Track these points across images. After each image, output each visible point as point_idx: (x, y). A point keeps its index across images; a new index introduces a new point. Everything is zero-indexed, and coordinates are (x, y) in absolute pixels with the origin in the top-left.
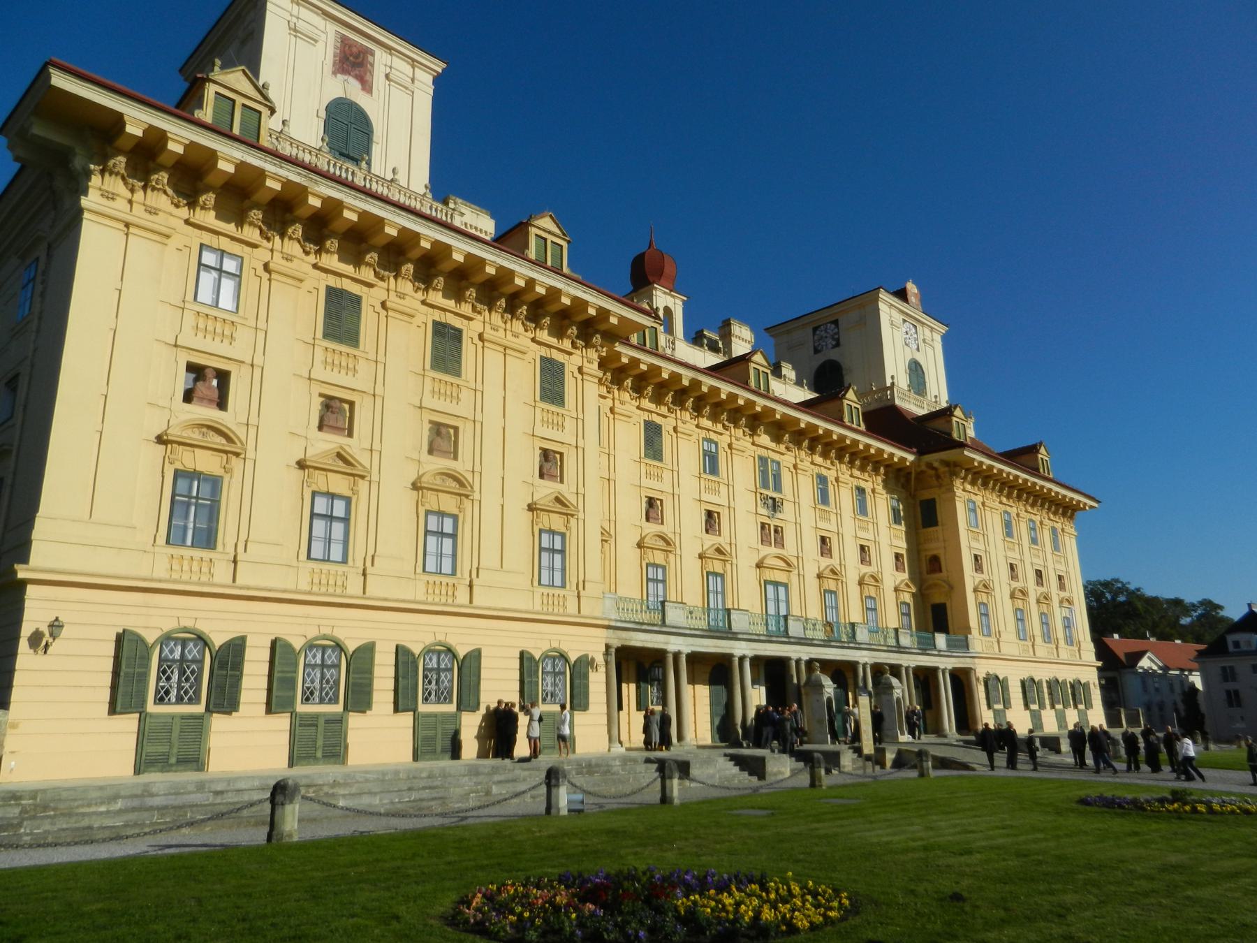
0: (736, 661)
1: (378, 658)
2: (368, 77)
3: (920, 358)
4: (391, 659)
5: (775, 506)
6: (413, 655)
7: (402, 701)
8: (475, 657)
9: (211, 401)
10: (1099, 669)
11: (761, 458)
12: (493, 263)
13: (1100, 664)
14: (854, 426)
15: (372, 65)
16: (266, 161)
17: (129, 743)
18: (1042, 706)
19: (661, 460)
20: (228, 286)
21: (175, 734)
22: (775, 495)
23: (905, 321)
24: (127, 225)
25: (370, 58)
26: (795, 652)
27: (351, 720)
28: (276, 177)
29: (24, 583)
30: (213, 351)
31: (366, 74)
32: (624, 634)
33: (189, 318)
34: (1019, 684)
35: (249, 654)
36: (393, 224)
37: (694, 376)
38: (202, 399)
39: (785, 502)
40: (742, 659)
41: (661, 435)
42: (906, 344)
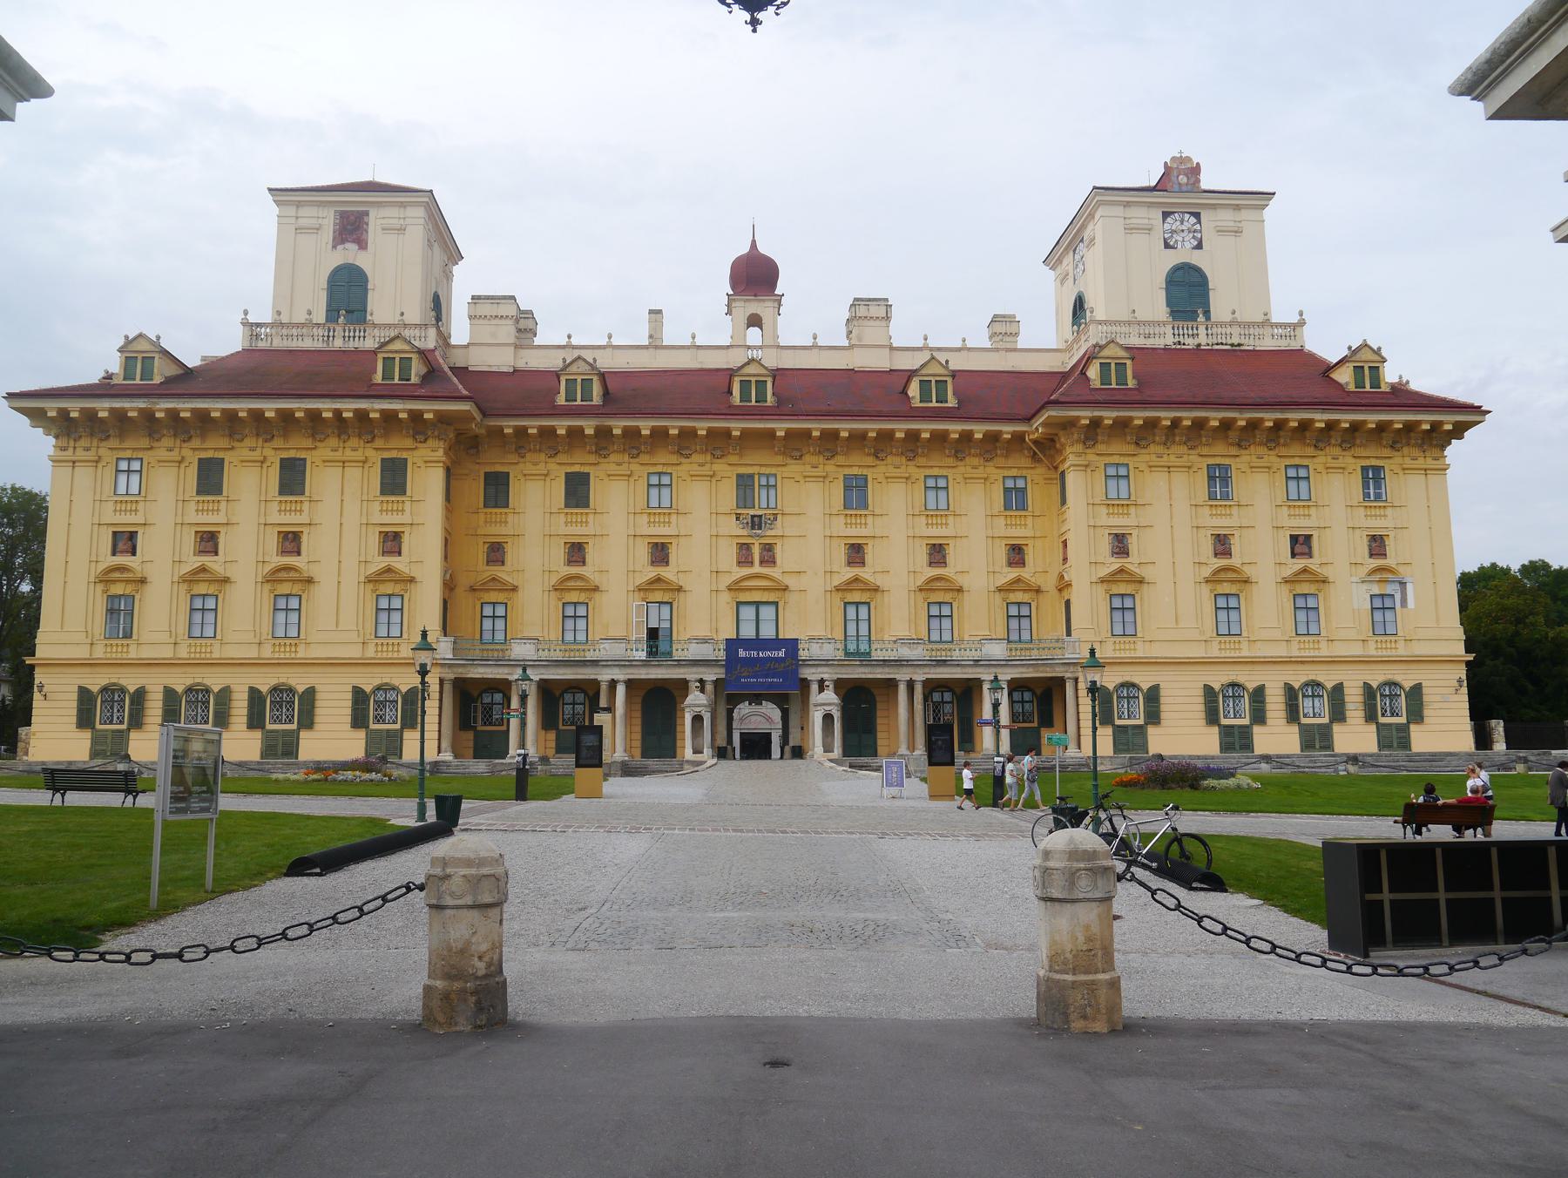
0: (604, 688)
1: (235, 696)
2: (364, 237)
3: (1196, 259)
4: (246, 696)
5: (756, 523)
6: (260, 692)
7: (255, 721)
8: (310, 693)
9: (127, 552)
10: (1468, 663)
11: (739, 476)
12: (299, 409)
13: (1471, 657)
14: (934, 404)
15: (367, 224)
16: (123, 402)
17: (87, 744)
18: (1259, 717)
19: (587, 506)
20: (135, 478)
21: (109, 741)
22: (760, 513)
23: (1166, 215)
24: (74, 462)
25: (366, 220)
26: (696, 673)
27: (131, 734)
28: (132, 409)
29: (32, 667)
30: (127, 520)
31: (362, 234)
32: (460, 670)
33: (110, 506)
34: (1201, 692)
35: (150, 696)
36: (216, 410)
37: (598, 423)
38: (122, 552)
39: (779, 517)
40: (613, 684)
41: (589, 484)
42: (1167, 246)
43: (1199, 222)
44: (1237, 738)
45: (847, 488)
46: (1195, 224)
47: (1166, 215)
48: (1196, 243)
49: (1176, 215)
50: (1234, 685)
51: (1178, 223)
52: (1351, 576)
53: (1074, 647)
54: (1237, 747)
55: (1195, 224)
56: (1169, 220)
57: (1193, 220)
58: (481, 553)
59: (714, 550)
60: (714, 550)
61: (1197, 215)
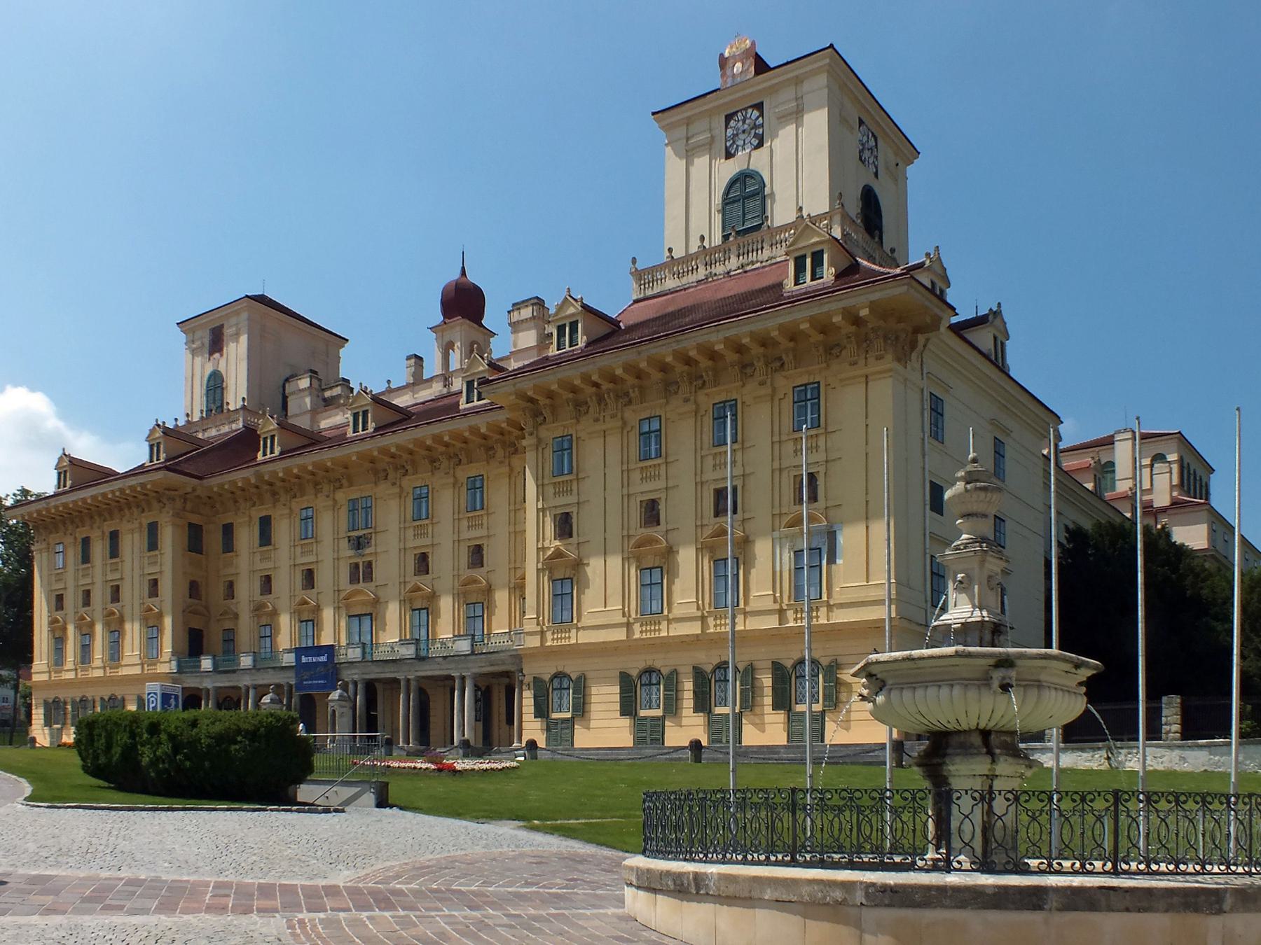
43: (762, 115)
44: (649, 733)
45: (353, 511)
46: (758, 118)
47: (729, 118)
48: (755, 142)
49: (739, 114)
50: (649, 671)
51: (741, 123)
52: (773, 530)
53: (520, 639)
54: (648, 740)
55: (758, 118)
56: (732, 123)
57: (756, 113)
58: (221, 589)
59: (336, 571)
60: (336, 571)
61: (759, 107)
